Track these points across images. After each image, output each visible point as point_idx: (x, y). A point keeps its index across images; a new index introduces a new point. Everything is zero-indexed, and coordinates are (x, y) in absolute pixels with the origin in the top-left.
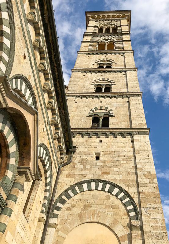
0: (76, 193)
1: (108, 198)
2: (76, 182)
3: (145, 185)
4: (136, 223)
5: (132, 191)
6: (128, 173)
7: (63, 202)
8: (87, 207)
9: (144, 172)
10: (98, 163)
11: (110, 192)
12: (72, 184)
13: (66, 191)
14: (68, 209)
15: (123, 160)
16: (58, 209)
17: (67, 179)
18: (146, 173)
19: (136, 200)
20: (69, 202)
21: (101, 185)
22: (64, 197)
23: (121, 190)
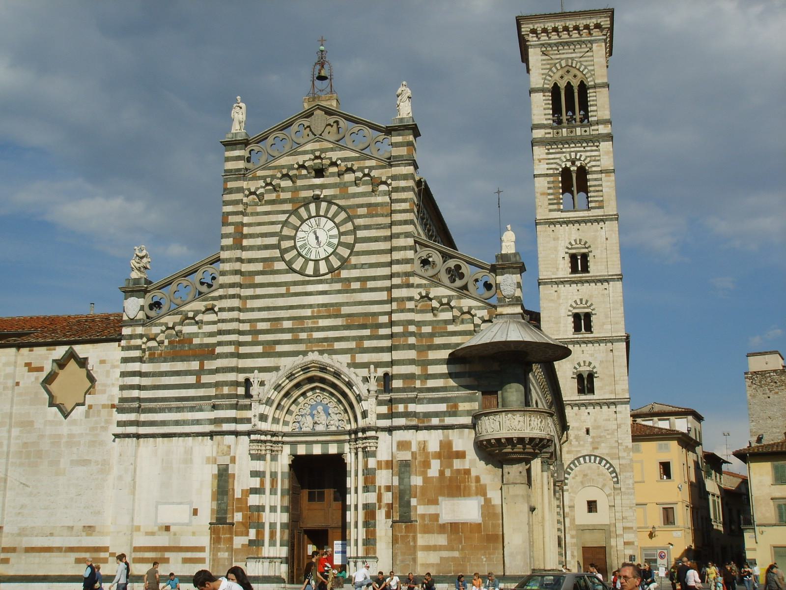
0: (576, 466)
1: (598, 468)
2: (576, 457)
3: (623, 458)
4: (617, 486)
5: (614, 463)
6: (612, 448)
7: (569, 473)
8: (585, 475)
9: (622, 447)
10: (589, 439)
11: (600, 463)
12: (573, 459)
13: (569, 465)
14: (573, 478)
15: (608, 434)
16: (567, 479)
17: (568, 455)
18: (625, 447)
19: (618, 470)
20: (573, 473)
21: (593, 458)
22: (568, 470)
23: (607, 462)
